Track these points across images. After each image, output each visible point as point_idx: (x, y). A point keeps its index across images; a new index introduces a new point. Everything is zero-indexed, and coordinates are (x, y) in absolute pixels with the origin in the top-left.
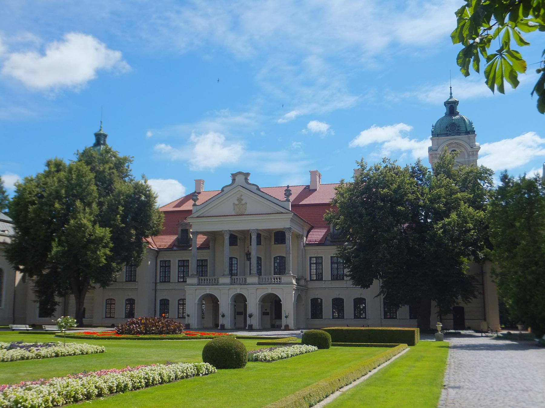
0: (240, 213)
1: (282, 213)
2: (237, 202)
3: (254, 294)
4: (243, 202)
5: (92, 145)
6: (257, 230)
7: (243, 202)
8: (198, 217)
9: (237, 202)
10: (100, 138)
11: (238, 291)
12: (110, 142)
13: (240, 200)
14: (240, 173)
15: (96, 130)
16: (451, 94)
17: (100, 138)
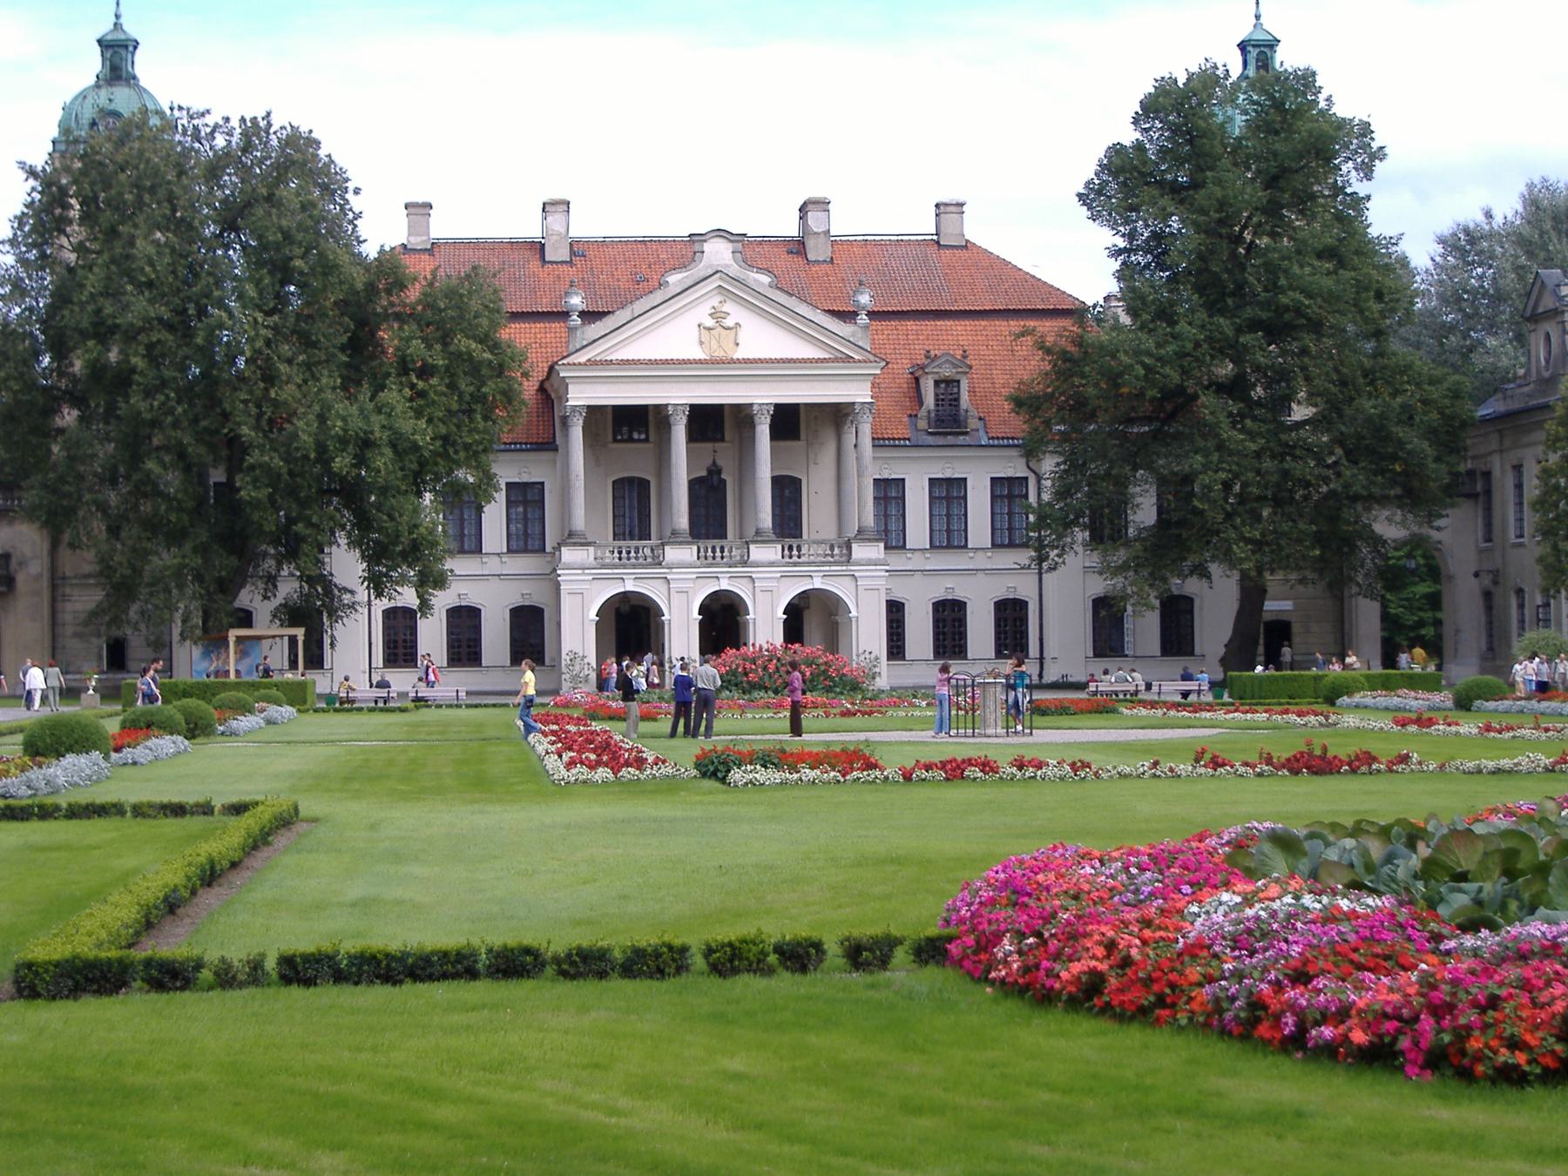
0: (719, 354)
1: (848, 359)
2: (710, 323)
3: (767, 591)
4: (729, 322)
5: (92, 80)
6: (777, 406)
7: (729, 322)
8: (592, 363)
9: (710, 323)
10: (117, 54)
11: (724, 585)
12: (144, 66)
13: (717, 315)
14: (720, 233)
15: (104, 27)
16: (1258, 17)
17: (117, 54)
